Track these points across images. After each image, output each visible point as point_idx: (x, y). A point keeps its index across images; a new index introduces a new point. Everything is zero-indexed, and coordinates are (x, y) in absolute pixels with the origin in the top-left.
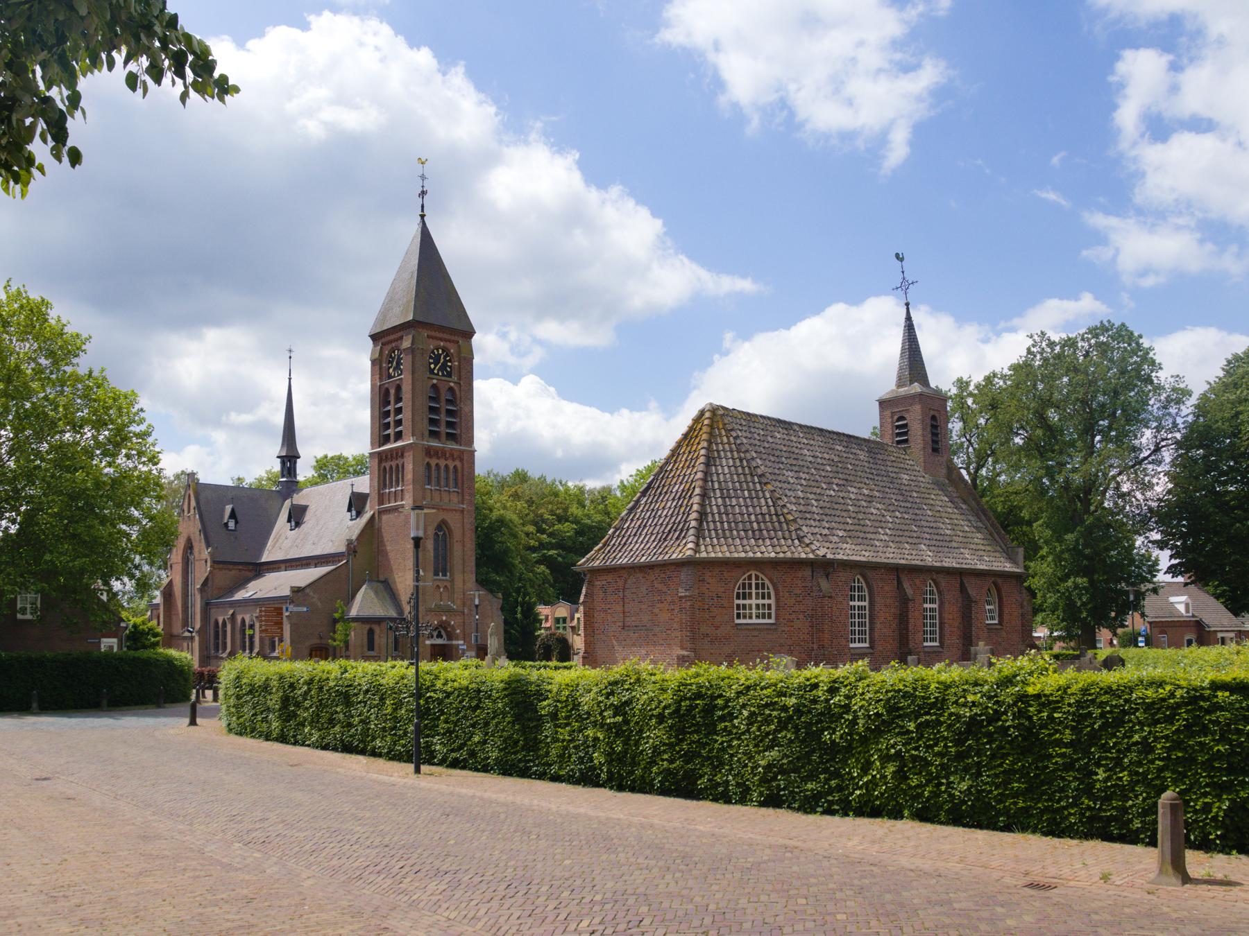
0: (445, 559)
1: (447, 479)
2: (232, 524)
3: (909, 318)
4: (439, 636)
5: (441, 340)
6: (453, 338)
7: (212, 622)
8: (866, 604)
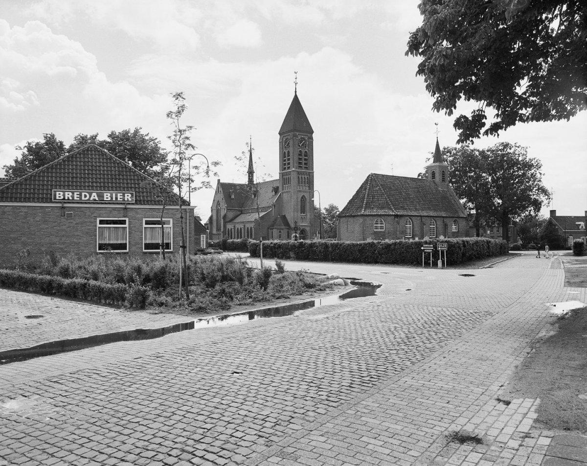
0: (304, 208)
1: (305, 182)
3: (437, 142)
5: (302, 135)
7: (227, 229)
8: (411, 226)
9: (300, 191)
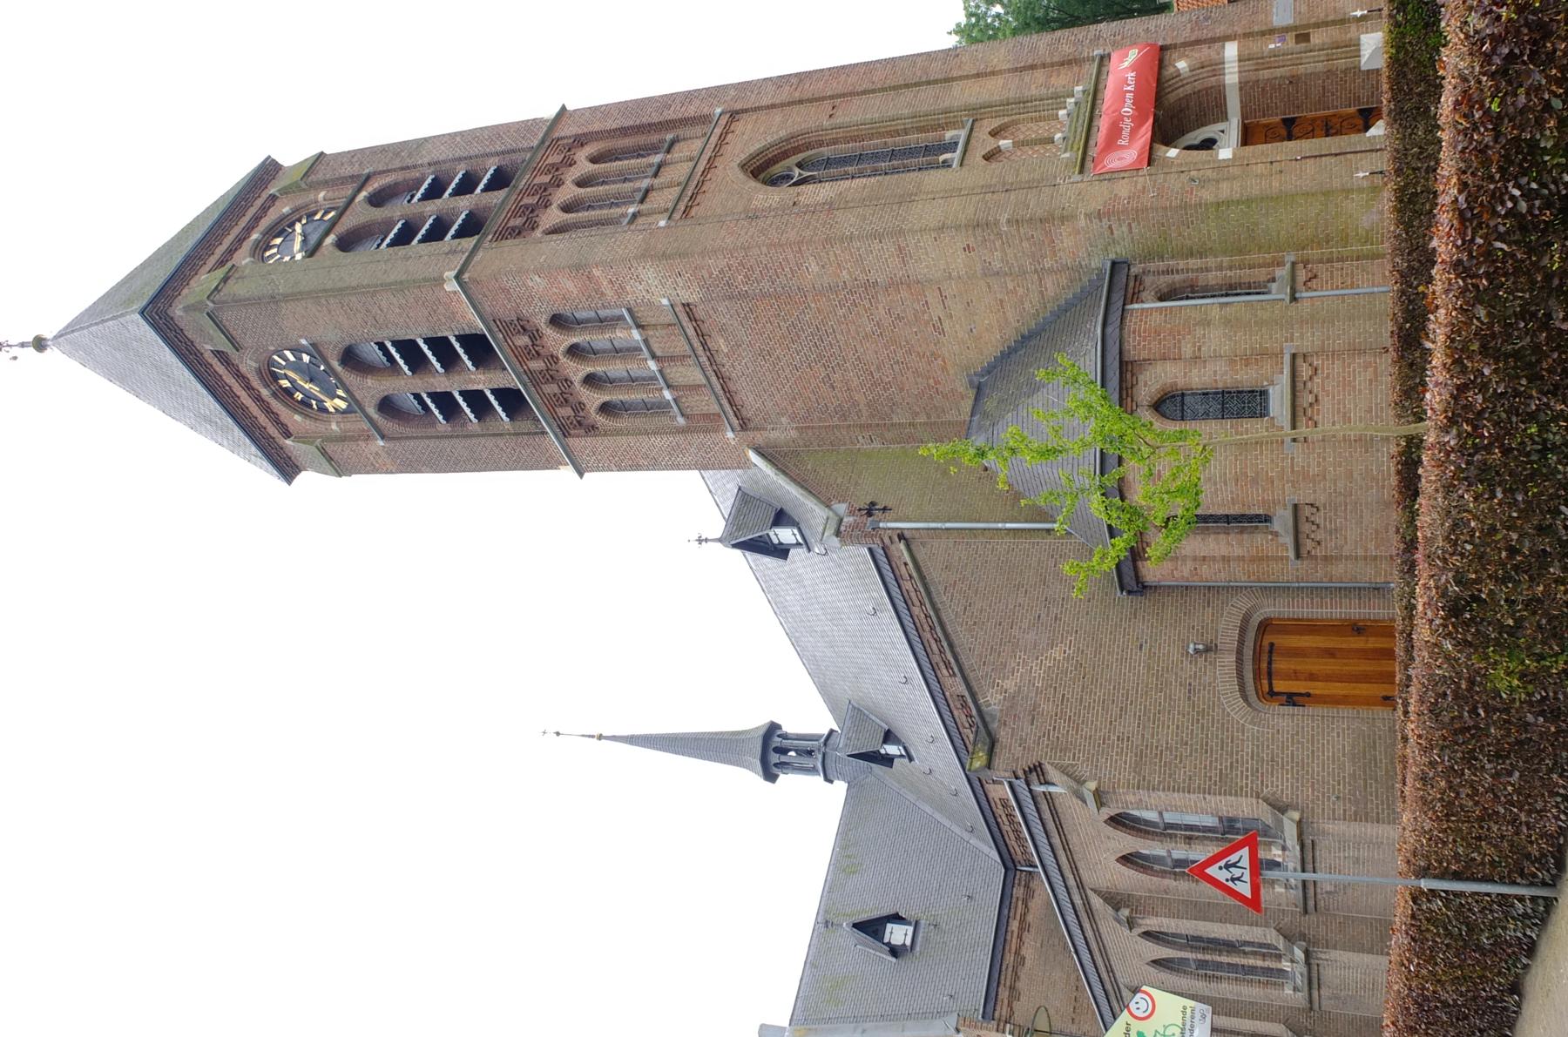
2: (898, 934)
5: (240, 241)
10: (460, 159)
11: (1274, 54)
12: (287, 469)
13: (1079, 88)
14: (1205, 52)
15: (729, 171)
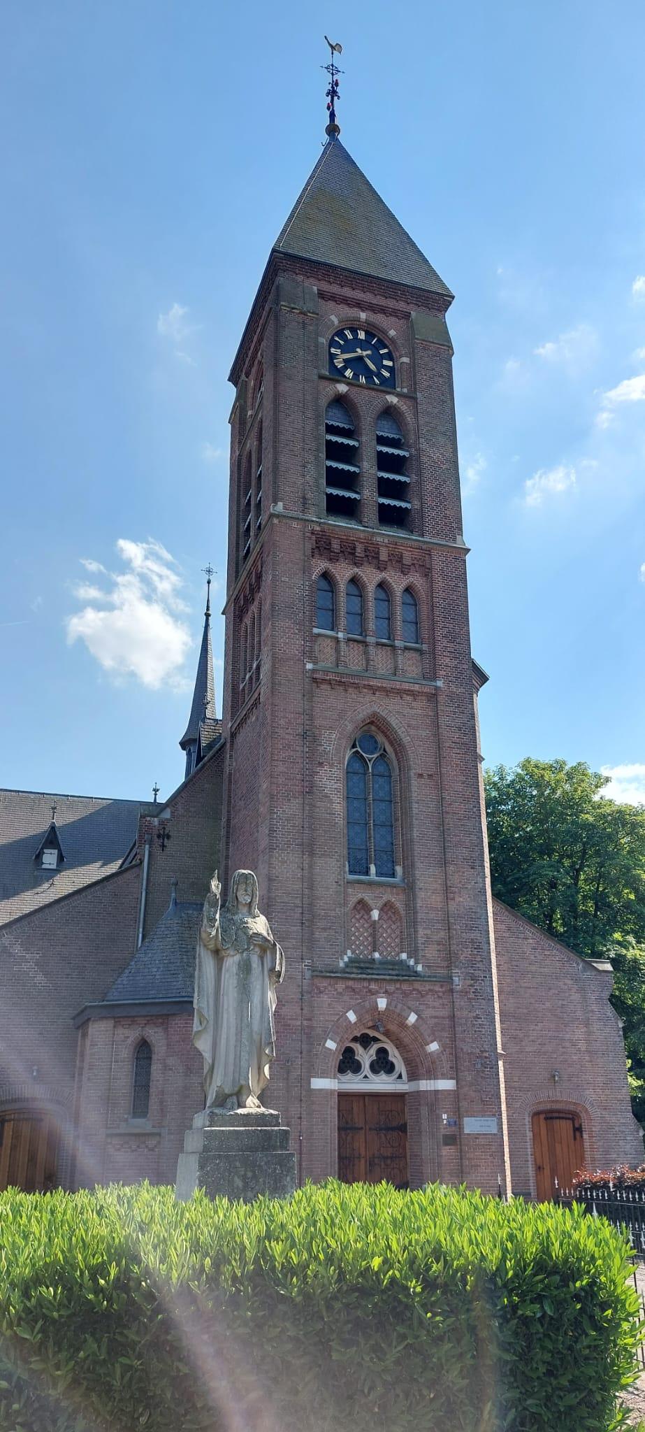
4: (382, 1064)
5: (359, 305)
6: (391, 303)
9: (342, 683)
10: (419, 474)
11: (439, 1118)
12: (234, 378)
13: (420, 968)
14: (446, 1066)
15: (366, 706)
